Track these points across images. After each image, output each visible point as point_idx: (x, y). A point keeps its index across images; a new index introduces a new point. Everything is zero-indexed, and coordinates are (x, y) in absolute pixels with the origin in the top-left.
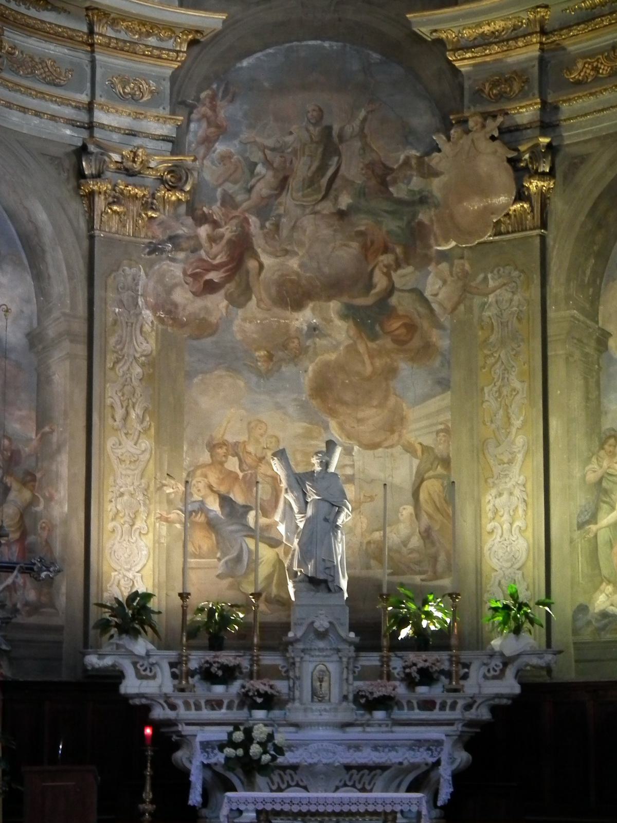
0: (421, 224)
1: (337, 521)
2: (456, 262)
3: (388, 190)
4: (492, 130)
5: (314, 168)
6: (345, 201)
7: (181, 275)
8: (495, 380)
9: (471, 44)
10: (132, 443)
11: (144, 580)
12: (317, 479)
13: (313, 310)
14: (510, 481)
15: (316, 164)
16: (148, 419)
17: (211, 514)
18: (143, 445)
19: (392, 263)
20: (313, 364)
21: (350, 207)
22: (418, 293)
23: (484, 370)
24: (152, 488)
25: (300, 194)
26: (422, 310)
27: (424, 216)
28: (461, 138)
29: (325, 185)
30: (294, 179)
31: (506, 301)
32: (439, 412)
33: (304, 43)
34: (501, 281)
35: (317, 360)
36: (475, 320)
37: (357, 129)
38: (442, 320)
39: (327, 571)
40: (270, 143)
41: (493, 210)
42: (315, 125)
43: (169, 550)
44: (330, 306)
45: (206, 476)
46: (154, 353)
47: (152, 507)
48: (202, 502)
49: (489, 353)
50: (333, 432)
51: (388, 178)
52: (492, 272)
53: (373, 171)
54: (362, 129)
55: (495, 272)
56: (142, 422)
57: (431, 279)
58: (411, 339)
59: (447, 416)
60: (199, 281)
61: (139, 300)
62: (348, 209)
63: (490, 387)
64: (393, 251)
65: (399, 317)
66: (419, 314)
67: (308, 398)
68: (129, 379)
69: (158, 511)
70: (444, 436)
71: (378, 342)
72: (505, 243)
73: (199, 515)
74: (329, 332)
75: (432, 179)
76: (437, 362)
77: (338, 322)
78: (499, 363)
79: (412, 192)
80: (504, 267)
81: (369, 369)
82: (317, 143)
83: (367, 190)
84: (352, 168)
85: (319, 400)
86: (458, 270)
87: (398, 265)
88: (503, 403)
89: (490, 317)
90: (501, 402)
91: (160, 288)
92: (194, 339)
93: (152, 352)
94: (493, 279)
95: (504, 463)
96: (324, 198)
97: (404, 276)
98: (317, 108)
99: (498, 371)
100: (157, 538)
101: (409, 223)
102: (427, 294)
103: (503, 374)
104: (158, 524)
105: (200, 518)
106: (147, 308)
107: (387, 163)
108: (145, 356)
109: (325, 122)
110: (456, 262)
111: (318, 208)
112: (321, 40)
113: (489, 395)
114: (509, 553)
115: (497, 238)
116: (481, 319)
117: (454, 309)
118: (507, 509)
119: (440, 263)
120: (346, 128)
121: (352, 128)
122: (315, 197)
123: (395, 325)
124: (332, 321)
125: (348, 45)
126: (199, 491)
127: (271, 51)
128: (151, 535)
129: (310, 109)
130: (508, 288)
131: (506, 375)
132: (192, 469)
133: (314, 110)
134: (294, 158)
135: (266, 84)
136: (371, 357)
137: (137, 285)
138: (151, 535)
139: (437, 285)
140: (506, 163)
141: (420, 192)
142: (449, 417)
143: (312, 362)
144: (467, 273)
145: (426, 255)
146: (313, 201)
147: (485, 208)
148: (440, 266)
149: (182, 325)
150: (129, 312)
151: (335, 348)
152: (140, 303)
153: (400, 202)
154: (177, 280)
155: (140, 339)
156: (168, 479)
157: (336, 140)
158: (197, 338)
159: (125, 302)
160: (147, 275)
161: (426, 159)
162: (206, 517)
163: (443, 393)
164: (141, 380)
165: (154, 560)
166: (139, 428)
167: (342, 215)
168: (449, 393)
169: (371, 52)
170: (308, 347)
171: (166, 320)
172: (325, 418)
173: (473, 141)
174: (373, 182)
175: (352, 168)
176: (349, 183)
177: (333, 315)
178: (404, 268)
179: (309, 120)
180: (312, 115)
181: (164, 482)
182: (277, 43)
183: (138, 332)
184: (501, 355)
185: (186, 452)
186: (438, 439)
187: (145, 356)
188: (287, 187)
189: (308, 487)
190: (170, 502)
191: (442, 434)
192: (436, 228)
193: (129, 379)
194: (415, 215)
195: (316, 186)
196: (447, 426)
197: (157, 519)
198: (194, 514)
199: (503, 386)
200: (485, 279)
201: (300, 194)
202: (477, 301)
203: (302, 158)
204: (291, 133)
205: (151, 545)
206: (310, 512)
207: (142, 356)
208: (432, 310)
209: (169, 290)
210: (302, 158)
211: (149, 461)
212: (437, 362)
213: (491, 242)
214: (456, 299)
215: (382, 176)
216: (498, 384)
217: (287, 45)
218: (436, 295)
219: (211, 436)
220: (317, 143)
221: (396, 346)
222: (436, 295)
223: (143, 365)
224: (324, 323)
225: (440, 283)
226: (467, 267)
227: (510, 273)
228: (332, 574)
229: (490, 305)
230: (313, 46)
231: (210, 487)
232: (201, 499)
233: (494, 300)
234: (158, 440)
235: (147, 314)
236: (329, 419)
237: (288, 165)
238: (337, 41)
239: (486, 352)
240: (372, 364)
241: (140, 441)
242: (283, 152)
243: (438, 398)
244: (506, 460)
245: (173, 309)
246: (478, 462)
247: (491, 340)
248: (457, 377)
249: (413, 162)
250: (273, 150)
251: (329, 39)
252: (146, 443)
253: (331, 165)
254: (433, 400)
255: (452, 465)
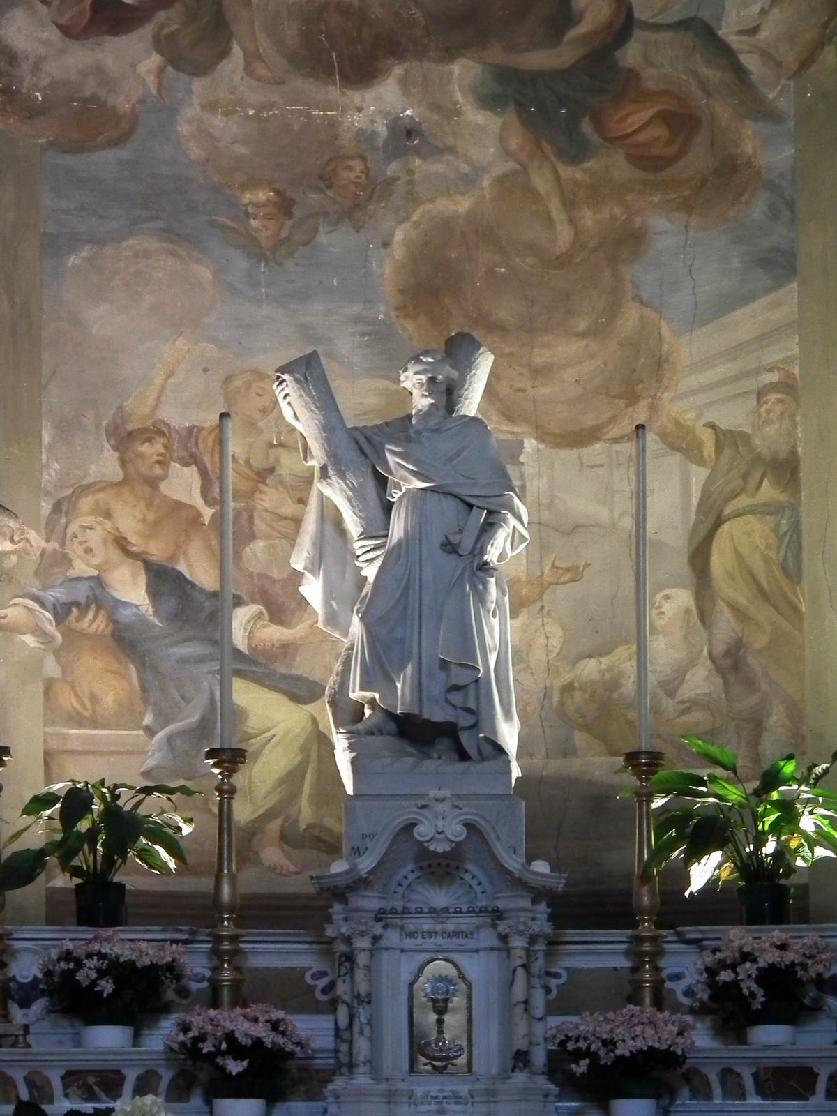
13: (404, 83)
17: (125, 614)
20: (408, 225)
26: (713, 75)
32: (765, 339)
35: (415, 217)
38: (771, 96)
44: (451, 73)
45: (108, 515)
48: (98, 581)
59: (792, 347)
65: (647, 96)
66: (702, 84)
67: (393, 313)
70: (780, 401)
71: (588, 164)
73: (90, 615)
74: (450, 141)
77: (475, 116)
81: (564, 236)
102: (728, 31)
105: (94, 623)
123: (636, 117)
124: (459, 113)
126: (89, 551)
136: (569, 204)
142: (797, 351)
143: (400, 222)
151: (469, 181)
162: (111, 619)
168: (795, 285)
170: (395, 179)
177: (459, 97)
186: (763, 410)
191: (773, 397)
196: (790, 375)
198: (74, 610)
208: (740, 72)
212: (758, 209)
218: (754, 31)
219: (120, 408)
221: (640, 175)
222: (754, 31)
231: (121, 543)
232: (95, 573)
240: (571, 221)
243: (763, 302)
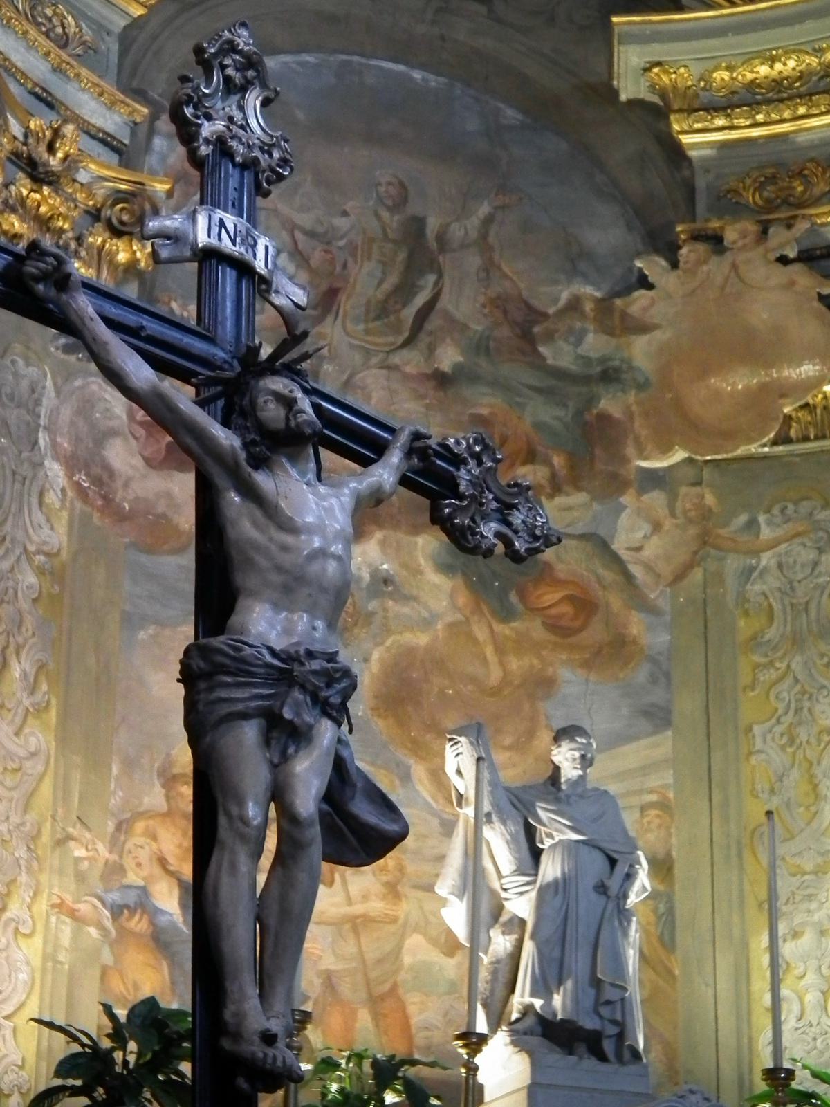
0: (604, 418)
1: (626, 897)
2: (683, 490)
3: (536, 351)
4: (782, 246)
5: (387, 286)
6: (449, 357)
7: (124, 417)
8: (780, 712)
9: (724, 102)
10: (10, 730)
11: (20, 1039)
12: (568, 796)
13: (383, 544)
14: (819, 909)
15: (393, 280)
16: (44, 687)
17: (162, 920)
18: (33, 740)
19: (544, 482)
20: (382, 648)
21: (458, 368)
22: (601, 545)
23: (752, 694)
24: (46, 838)
25: (361, 327)
26: (608, 576)
27: (610, 404)
28: (705, 262)
29: (411, 320)
30: (348, 298)
31: (803, 566)
32: (646, 769)
33: (374, 62)
34: (789, 528)
35: (388, 643)
36: (730, 599)
37: (474, 234)
38: (652, 596)
39: (605, 1011)
40: (305, 220)
41: (784, 391)
42: (393, 209)
43: (73, 979)
44: (416, 543)
45: (154, 838)
46: (64, 555)
47: (44, 878)
48: (144, 891)
49: (763, 660)
50: (420, 788)
51: (536, 329)
52: (768, 511)
53: (505, 312)
54: (484, 236)
55: (776, 511)
56: (32, 690)
57: (624, 519)
58: (580, 630)
59: (668, 777)
60: (158, 441)
61: (40, 435)
62: (453, 373)
63: (768, 725)
64: (547, 462)
65: (558, 583)
66: (599, 580)
67: (369, 712)
68: (11, 591)
69: (56, 890)
70: (658, 816)
71: (515, 624)
72: (798, 459)
73: (137, 918)
74: (415, 592)
75: (633, 337)
76: (641, 674)
77: (435, 578)
78: (789, 680)
79: (587, 361)
80: (796, 503)
81: (495, 675)
82: (395, 242)
83: (492, 344)
84: (464, 303)
85: (391, 721)
86: (688, 506)
87: (556, 487)
88: (800, 755)
89: (764, 594)
90: (794, 754)
91: (83, 427)
92: (141, 551)
93: (59, 550)
94: (769, 523)
95: (804, 873)
96: (407, 343)
97: (570, 508)
98: (394, 181)
99: (785, 694)
100: (50, 949)
101: (579, 413)
102: (619, 545)
103: (797, 701)
104: (53, 919)
105: (138, 924)
106: (56, 458)
107: (535, 303)
108: (47, 555)
109: (414, 208)
110: (683, 490)
111: (396, 359)
112: (406, 63)
113: (765, 741)
114: (822, 1053)
115: (780, 449)
116: (742, 598)
117: (679, 577)
118: (813, 964)
119: (646, 492)
120: (453, 226)
121: (465, 229)
122: (391, 339)
123: (550, 596)
124: (421, 573)
125: (458, 85)
126: (139, 865)
127: (310, 58)
128: (38, 940)
129: (383, 180)
130: (806, 540)
131: (807, 704)
132: (127, 815)
133: (389, 184)
134: (350, 261)
135: (300, 115)
136: (500, 651)
137: (38, 403)
138: (38, 940)
139: (641, 532)
140: (816, 304)
141: (603, 360)
142: (671, 781)
143: (377, 645)
144: (710, 510)
145: (614, 477)
146: (386, 344)
147: (764, 388)
148: (645, 497)
149: (122, 517)
150: (21, 452)
151: (427, 624)
152: (42, 443)
153: (560, 374)
154: (113, 423)
155: (39, 517)
156: (78, 826)
157: (433, 245)
158: (150, 551)
159: (13, 429)
160: (58, 392)
161: (618, 302)
162: (152, 923)
163: (654, 733)
164: (35, 600)
165: (42, 1000)
166: (26, 703)
167: (442, 380)
168: (669, 733)
169: (501, 105)
170: (373, 614)
171: (91, 494)
172: (404, 759)
173: (734, 267)
174: (505, 332)
175: (464, 303)
176: (455, 326)
177: (422, 561)
178: (568, 495)
179: (380, 200)
180: (387, 192)
181: (71, 830)
182: (318, 49)
183: (35, 501)
184: (793, 666)
185: (117, 779)
186: (645, 820)
187: (47, 555)
188: (335, 308)
189: (541, 813)
190: (81, 877)
191: (653, 812)
192: (640, 427)
193: (11, 591)
194: (591, 400)
195: (392, 318)
196: (665, 797)
197: (53, 906)
198: (126, 911)
199: (800, 723)
200: (752, 524)
201: (361, 327)
202: (733, 564)
203: (366, 263)
204: (345, 214)
205: (37, 962)
206: (551, 868)
207: (39, 552)
208: (628, 577)
209: (103, 436)
210: (366, 263)
211: (41, 779)
212: (641, 674)
213: (765, 457)
214: (682, 556)
215: (525, 327)
216: (789, 719)
217: (344, 57)
218: (639, 549)
219: (168, 755)
220: (395, 242)
221: (553, 638)
222: (639, 549)
223: (40, 571)
224: (405, 573)
225: (646, 528)
226: (710, 499)
227: (811, 514)
228: (619, 1017)
229: (765, 570)
230: (390, 71)
231: (162, 862)
232: (142, 883)
233: (773, 562)
234: (63, 739)
235: (55, 470)
236: (412, 762)
237: (338, 269)
238: (438, 74)
239: (757, 658)
240: (501, 663)
241: (27, 730)
242: (329, 243)
243: (644, 742)
244: (809, 867)
245: (105, 477)
246: (741, 868)
247: (767, 637)
248: (687, 704)
249: (588, 307)
250: (311, 234)
251: (423, 67)
252: (39, 737)
253: (422, 288)
254: (634, 746)
255: (677, 871)
